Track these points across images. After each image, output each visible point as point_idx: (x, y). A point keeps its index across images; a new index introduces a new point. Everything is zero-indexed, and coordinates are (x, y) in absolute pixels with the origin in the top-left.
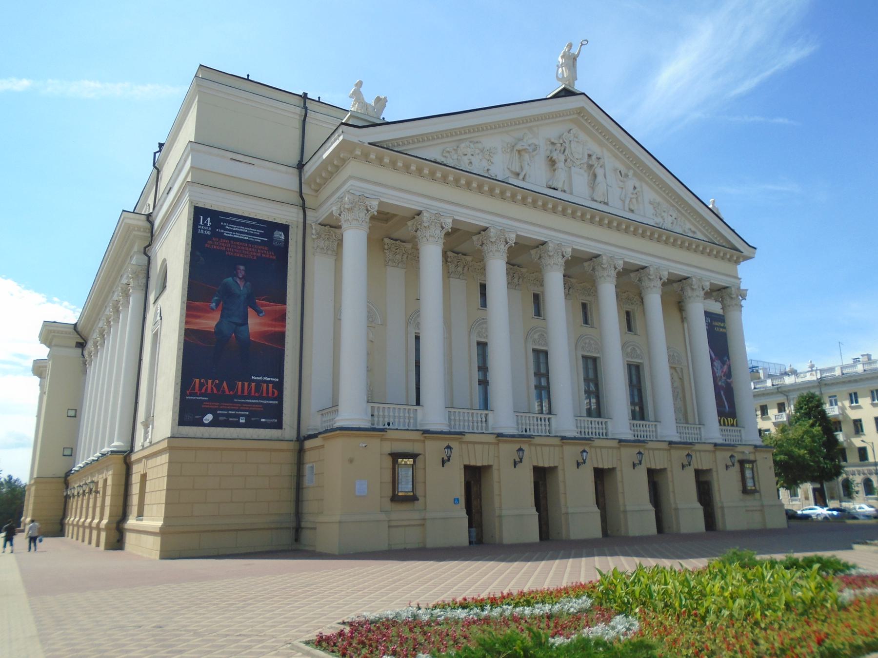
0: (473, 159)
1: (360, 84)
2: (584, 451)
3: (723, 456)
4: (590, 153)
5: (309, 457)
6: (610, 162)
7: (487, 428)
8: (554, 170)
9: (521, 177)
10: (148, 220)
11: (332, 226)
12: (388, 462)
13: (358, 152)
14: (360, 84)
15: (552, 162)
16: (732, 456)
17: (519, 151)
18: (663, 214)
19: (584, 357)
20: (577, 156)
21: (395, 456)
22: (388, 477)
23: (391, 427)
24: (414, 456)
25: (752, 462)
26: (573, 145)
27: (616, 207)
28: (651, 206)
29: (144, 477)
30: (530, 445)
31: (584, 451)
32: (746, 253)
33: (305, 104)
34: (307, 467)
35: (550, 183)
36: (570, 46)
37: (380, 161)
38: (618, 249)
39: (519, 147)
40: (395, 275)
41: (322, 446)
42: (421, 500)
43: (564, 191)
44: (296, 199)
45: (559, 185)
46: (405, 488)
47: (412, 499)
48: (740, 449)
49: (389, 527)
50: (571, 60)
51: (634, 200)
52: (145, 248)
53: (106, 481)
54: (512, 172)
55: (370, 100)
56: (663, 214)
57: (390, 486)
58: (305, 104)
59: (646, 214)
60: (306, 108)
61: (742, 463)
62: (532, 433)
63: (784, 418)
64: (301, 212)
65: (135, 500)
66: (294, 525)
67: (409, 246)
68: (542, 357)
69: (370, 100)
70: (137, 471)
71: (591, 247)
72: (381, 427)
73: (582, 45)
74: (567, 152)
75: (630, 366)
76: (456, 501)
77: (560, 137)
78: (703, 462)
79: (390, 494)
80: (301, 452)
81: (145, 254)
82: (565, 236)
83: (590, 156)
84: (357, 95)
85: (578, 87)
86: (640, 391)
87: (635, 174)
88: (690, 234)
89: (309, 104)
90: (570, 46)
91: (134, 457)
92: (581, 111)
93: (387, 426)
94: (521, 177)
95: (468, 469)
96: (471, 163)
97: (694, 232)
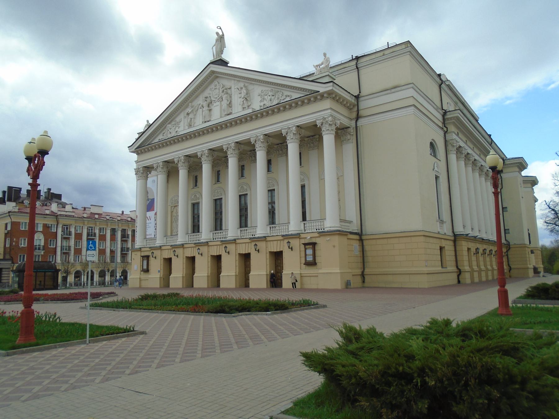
2: (199, 249)
17: (188, 114)
18: (266, 97)
25: (314, 245)
36: (217, 33)
37: (142, 153)
49: (140, 280)
59: (257, 105)
88: (288, 99)
90: (217, 33)
92: (213, 72)
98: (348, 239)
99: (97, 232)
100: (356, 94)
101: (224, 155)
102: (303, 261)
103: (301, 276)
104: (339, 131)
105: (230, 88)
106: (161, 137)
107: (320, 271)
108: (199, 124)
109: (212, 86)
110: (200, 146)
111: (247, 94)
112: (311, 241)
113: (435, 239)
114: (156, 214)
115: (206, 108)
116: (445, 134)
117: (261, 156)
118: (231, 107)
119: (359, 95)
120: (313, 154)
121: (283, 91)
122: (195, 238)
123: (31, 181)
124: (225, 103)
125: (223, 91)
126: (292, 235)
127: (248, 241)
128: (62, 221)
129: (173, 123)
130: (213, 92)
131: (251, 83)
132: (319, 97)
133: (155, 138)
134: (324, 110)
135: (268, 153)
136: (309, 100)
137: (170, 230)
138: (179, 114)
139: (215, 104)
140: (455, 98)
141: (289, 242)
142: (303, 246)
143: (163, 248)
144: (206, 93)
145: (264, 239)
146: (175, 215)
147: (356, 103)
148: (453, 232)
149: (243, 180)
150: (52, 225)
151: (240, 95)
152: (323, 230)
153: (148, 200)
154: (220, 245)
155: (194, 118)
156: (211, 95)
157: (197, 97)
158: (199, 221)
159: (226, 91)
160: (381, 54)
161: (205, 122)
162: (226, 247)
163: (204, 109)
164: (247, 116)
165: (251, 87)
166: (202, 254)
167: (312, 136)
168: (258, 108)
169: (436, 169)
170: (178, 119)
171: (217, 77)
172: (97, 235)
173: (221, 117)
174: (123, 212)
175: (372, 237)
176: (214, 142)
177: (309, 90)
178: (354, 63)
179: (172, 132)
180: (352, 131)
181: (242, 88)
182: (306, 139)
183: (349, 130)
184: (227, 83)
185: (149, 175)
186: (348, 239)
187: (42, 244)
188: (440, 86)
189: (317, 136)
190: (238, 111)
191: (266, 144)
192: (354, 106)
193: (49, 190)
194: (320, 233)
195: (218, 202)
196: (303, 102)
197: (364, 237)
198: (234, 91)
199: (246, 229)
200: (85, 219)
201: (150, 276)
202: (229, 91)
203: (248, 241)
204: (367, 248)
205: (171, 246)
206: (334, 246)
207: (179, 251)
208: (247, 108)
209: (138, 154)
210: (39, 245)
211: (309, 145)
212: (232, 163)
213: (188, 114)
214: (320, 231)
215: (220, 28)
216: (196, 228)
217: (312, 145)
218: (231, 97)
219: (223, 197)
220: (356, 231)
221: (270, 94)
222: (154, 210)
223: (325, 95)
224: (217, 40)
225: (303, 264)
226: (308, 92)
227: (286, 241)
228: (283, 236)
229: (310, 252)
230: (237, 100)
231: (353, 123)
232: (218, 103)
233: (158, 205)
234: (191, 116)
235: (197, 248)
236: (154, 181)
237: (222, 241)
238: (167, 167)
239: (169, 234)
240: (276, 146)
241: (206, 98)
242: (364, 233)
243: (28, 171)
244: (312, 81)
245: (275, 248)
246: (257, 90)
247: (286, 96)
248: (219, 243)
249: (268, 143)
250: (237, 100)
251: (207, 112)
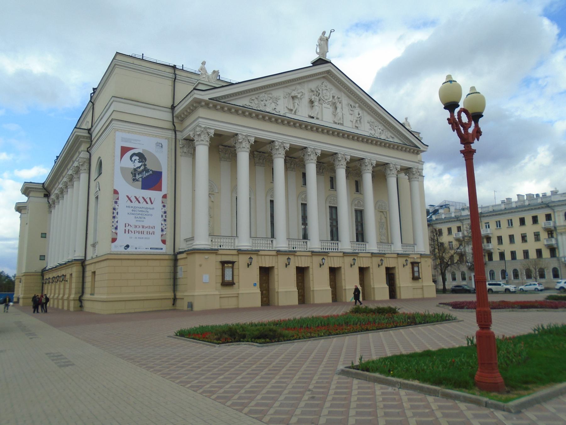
1: (204, 63)
2: (323, 259)
3: (402, 261)
4: (334, 95)
5: (180, 263)
6: (345, 100)
7: (272, 247)
8: (313, 106)
9: (293, 112)
10: (89, 133)
11: (190, 142)
12: (220, 266)
13: (203, 104)
14: (204, 63)
15: (311, 102)
16: (406, 260)
17: (293, 98)
18: (376, 128)
19: (330, 207)
20: (326, 98)
21: (223, 263)
22: (219, 272)
23: (222, 248)
24: (233, 263)
25: (418, 263)
26: (325, 91)
27: (348, 127)
28: (369, 124)
29: (94, 273)
30: (295, 255)
31: (323, 259)
32: (422, 149)
33: (175, 71)
34: (179, 268)
35: (310, 114)
36: (324, 33)
38: (346, 150)
39: (293, 95)
40: (225, 166)
41: (186, 258)
42: (237, 284)
43: (318, 119)
44: (169, 125)
46: (228, 278)
47: (231, 284)
48: (411, 256)
50: (324, 41)
52: (88, 148)
53: (71, 275)
54: (288, 109)
55: (210, 72)
56: (376, 128)
57: (221, 277)
58: (175, 71)
60: (175, 74)
61: (413, 264)
62: (296, 249)
63: (460, 235)
64: (174, 133)
65: (88, 285)
66: (173, 297)
67: (233, 149)
69: (210, 72)
70: (89, 270)
71: (333, 149)
72: (216, 248)
74: (320, 95)
75: (356, 211)
76: (255, 285)
77: (317, 87)
78: (390, 263)
79: (221, 281)
80: (176, 260)
81: (88, 151)
82: (316, 144)
83: (333, 97)
84: (202, 69)
85: (329, 57)
86: (362, 225)
87: (360, 106)
88: (391, 140)
89: (177, 72)
90: (324, 33)
91: (87, 263)
92: (328, 72)
93: (219, 248)
94: (293, 112)
95: (261, 268)
96: (265, 105)
121: (389, 132)
134: (413, 162)
151: (351, 112)
164: (351, 135)
171: (324, 77)
176: (360, 152)
224: (321, 39)
234: (297, 101)
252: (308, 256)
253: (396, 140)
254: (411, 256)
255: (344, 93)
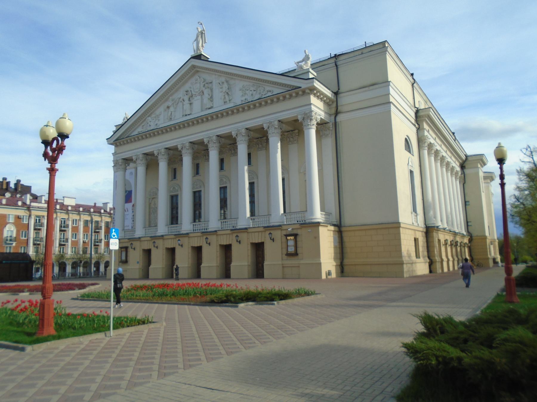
0: (152, 124)
2: (179, 240)
18: (247, 92)
25: (296, 235)
45: (184, 114)
48: (284, 227)
51: (226, 96)
59: (238, 99)
68: (222, 190)
73: (201, 24)
88: (269, 94)
92: (194, 67)
95: (144, 250)
97: (270, 91)
98: (328, 230)
99: (70, 223)
100: (335, 91)
101: (206, 148)
102: (285, 252)
103: (283, 267)
104: (320, 126)
105: (211, 83)
106: (140, 130)
107: (302, 262)
108: (179, 118)
109: (193, 80)
110: (181, 139)
111: (228, 89)
112: (292, 233)
113: (410, 231)
114: (133, 206)
115: (187, 101)
116: (417, 131)
117: (242, 149)
118: (212, 101)
119: (337, 92)
120: (293, 148)
122: (175, 229)
123: (49, 166)
124: (206, 96)
125: (204, 85)
126: (273, 226)
127: (229, 232)
128: (34, 213)
129: (153, 116)
130: (194, 85)
131: (232, 78)
132: (300, 93)
133: (135, 130)
135: (249, 147)
136: (291, 96)
137: (151, 221)
138: (158, 108)
139: (196, 98)
140: (424, 97)
141: (270, 233)
142: (284, 238)
143: (142, 239)
144: (187, 87)
145: (245, 230)
146: (153, 206)
147: (335, 99)
148: (425, 224)
149: (223, 173)
150: (23, 216)
151: (221, 90)
152: (304, 222)
153: (126, 191)
154: (200, 236)
155: (175, 111)
156: (192, 90)
157: (177, 91)
158: (177, 213)
159: (208, 84)
160: (360, 52)
161: (186, 115)
162: (207, 238)
163: (185, 103)
165: (232, 82)
166: (182, 246)
167: (292, 131)
168: (239, 103)
169: (410, 164)
170: (157, 112)
171: (198, 71)
172: (70, 227)
173: (202, 111)
174: (95, 204)
175: (350, 229)
177: (291, 86)
178: (333, 60)
179: (152, 124)
180: (331, 125)
181: (223, 83)
182: (286, 134)
183: (328, 124)
184: (208, 77)
185: (128, 167)
186: (328, 230)
187: (14, 235)
188: (413, 84)
189: (297, 131)
190: (219, 106)
191: (247, 138)
192: (333, 102)
193: (18, 181)
194: (302, 224)
195: (197, 194)
196: (284, 97)
197: (343, 229)
198: (215, 86)
199: (225, 220)
200: (58, 211)
201: (128, 267)
202: (210, 85)
203: (229, 232)
204: (346, 239)
205: (151, 237)
206: (315, 238)
207: (159, 242)
208: (228, 101)
209: (116, 146)
210: (11, 237)
211: (288, 139)
212: (214, 155)
213: (168, 107)
214: (301, 222)
215: (201, 24)
216: (174, 219)
217: (291, 139)
218: (212, 90)
219: (202, 189)
220: (335, 223)
221: (252, 89)
222: (131, 202)
223: (307, 91)
225: (284, 255)
226: (290, 87)
227: (268, 232)
228: (265, 227)
229: (291, 243)
230: (218, 95)
231: (333, 117)
232: (199, 97)
233: (139, 197)
234: (172, 109)
235: (178, 239)
236: (131, 173)
237: (203, 232)
238: (147, 160)
239: (147, 226)
240: (255, 140)
241: (187, 91)
242: (343, 224)
243: (45, 155)
244: (294, 77)
245: (257, 240)
246: (238, 85)
247: (268, 91)
248: (199, 234)
249: (249, 136)
250: (218, 95)
251: (189, 105)
252: (198, 237)
253: (277, 91)
254: (284, 227)
255: (215, 75)
